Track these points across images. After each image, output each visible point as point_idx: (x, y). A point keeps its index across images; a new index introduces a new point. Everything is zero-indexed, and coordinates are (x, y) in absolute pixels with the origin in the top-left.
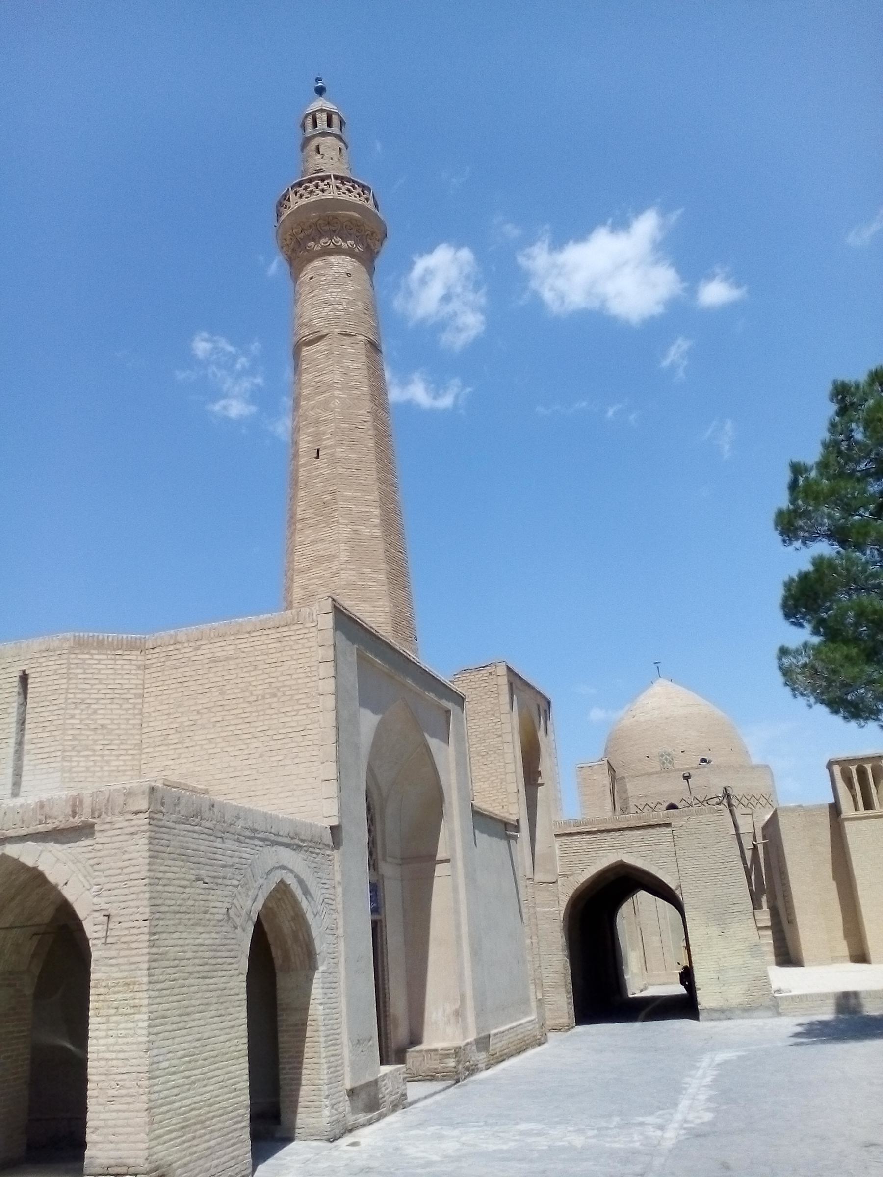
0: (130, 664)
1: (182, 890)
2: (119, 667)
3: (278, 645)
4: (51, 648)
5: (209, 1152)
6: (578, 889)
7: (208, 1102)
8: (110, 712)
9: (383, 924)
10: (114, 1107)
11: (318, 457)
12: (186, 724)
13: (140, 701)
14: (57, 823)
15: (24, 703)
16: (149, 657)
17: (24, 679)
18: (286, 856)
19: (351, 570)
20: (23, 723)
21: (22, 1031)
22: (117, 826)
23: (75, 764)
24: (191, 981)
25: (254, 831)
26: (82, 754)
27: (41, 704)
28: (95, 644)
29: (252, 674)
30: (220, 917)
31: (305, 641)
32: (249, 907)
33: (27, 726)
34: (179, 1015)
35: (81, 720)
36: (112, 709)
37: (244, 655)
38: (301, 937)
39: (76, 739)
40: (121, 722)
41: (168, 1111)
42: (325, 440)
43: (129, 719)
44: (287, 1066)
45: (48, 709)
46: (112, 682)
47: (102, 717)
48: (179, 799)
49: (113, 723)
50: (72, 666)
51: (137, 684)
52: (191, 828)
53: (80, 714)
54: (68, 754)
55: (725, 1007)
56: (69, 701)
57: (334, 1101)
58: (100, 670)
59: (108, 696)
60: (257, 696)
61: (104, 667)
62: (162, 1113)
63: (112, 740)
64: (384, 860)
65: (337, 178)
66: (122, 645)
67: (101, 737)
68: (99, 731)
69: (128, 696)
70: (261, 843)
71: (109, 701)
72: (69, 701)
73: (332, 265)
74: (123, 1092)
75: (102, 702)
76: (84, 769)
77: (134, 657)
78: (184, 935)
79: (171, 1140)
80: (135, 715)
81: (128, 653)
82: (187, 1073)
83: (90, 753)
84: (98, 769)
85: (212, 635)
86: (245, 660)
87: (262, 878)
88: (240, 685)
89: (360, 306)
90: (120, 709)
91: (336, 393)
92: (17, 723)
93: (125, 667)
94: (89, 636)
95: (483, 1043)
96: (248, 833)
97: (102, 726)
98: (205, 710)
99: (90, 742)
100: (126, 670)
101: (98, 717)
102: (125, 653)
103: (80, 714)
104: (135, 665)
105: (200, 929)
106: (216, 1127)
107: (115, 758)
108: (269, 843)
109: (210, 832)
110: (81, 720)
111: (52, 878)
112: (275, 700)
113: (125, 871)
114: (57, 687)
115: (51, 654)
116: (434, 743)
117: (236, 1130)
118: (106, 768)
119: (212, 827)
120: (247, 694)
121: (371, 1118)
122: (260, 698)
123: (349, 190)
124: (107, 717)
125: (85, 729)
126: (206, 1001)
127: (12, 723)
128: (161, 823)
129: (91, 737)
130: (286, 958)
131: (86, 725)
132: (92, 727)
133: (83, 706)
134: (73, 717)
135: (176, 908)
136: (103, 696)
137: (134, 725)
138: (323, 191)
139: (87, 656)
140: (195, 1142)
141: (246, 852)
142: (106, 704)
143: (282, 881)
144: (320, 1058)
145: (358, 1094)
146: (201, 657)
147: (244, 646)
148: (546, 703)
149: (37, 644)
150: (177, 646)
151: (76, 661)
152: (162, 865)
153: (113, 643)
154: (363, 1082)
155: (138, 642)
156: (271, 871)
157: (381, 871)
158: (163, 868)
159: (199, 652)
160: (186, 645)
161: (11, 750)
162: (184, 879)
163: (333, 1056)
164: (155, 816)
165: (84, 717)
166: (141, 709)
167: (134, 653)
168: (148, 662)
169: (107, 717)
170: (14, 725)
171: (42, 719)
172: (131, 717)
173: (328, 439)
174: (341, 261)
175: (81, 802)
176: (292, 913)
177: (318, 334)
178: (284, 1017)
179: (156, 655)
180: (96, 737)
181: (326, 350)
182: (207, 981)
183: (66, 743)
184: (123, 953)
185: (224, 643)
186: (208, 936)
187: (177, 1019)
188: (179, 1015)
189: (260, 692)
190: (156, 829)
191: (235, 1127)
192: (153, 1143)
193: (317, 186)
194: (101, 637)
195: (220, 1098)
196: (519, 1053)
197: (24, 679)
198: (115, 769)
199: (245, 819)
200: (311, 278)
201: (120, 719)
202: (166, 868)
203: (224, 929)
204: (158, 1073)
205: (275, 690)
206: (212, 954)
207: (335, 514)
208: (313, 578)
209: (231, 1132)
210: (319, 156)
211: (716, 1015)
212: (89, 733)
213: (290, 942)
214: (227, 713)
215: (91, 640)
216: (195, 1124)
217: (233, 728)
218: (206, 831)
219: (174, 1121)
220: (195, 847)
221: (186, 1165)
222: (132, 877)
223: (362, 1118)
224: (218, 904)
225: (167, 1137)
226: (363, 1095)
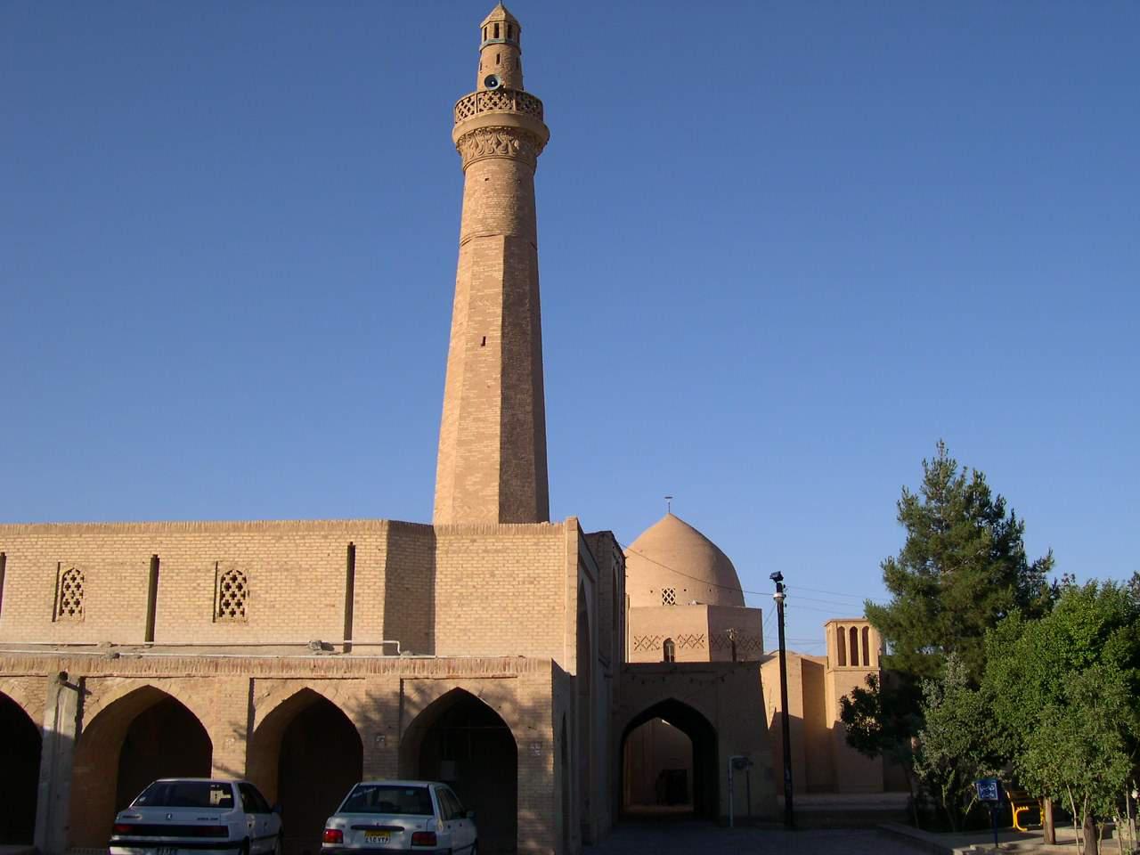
11: (484, 344)
60: (519, 582)
97: (407, 588)
112: (533, 586)
118: (410, 619)
120: (512, 579)
133: (396, 574)
159: (475, 544)
173: (494, 330)
181: (496, 249)
205: (532, 579)
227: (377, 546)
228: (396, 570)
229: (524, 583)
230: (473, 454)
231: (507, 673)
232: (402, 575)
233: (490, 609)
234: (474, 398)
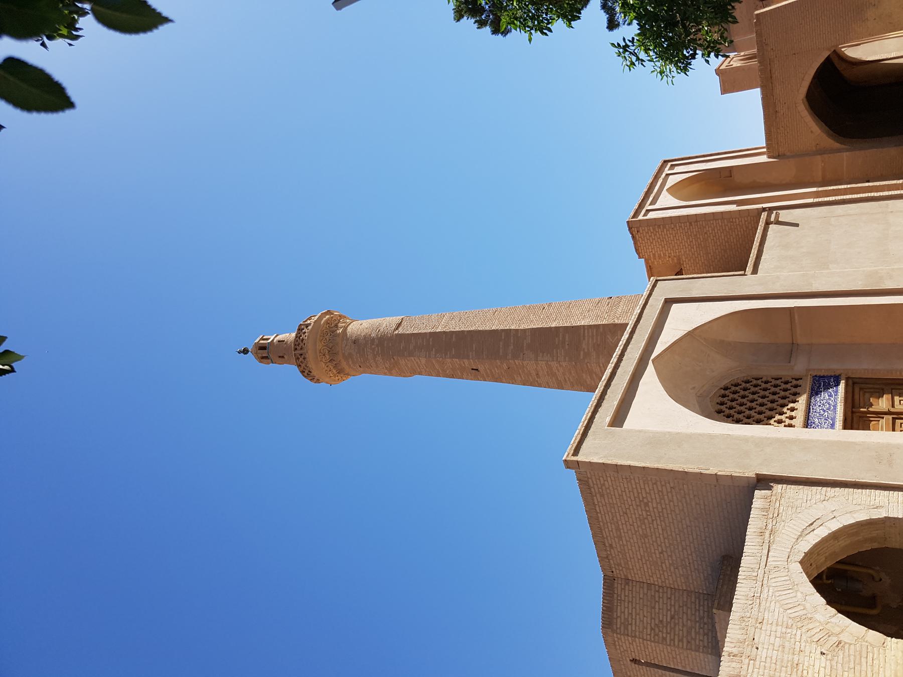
49: (670, 610)
54: (693, 647)
99: (685, 629)
118: (705, 620)
120: (646, 521)
132: (672, 625)
134: (664, 639)
139: (619, 620)
180: (681, 624)
212: (677, 629)
228: (652, 629)
232: (657, 622)
233: (683, 543)
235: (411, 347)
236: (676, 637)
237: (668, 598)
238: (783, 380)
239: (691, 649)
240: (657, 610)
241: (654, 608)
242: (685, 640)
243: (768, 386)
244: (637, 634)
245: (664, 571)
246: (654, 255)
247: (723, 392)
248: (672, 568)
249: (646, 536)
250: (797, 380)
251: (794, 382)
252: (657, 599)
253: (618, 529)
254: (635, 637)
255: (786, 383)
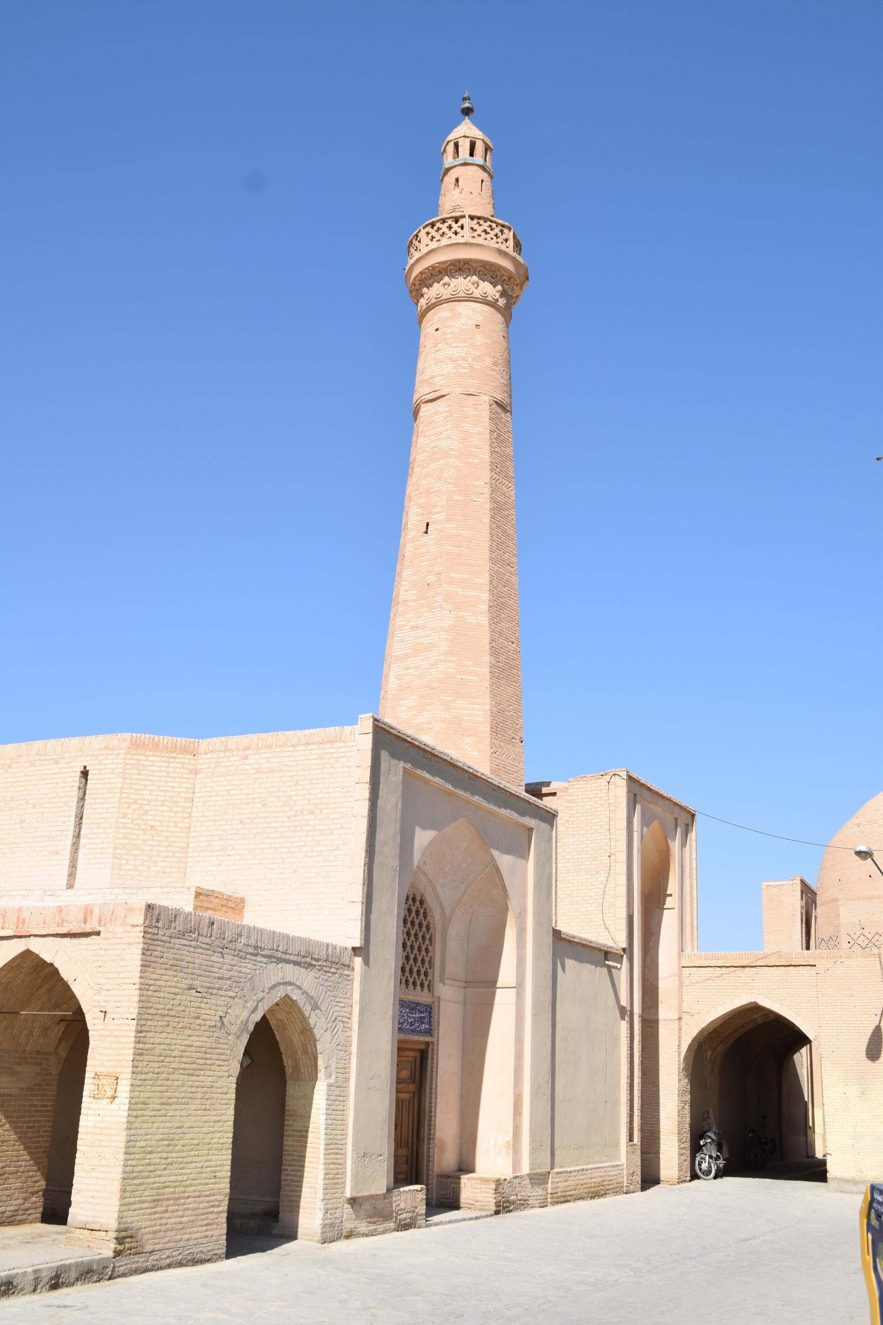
0: (183, 768)
1: (173, 996)
2: (172, 770)
3: (320, 761)
4: (110, 746)
5: (180, 1226)
6: (703, 1030)
7: (184, 1183)
8: (160, 813)
9: (435, 1047)
10: (94, 1175)
12: (229, 832)
13: (189, 805)
14: (72, 927)
15: (83, 799)
16: (201, 761)
17: (85, 774)
18: (290, 972)
19: (450, 661)
20: (81, 818)
21: (46, 1106)
22: (118, 936)
23: (124, 861)
24: (176, 1076)
25: (256, 948)
26: (131, 852)
27: (98, 801)
28: (150, 746)
29: (293, 788)
30: (213, 1023)
31: (345, 760)
32: (245, 1017)
33: (84, 821)
34: (161, 1104)
35: (133, 820)
36: (162, 812)
37: (287, 768)
38: (310, 1051)
39: (127, 838)
40: (171, 824)
41: (141, 1184)
42: (435, 513)
43: (178, 822)
44: (290, 1168)
45: (104, 806)
46: (163, 784)
47: (152, 818)
48: (176, 916)
50: (128, 766)
51: (188, 788)
52: (187, 943)
53: (132, 814)
54: (118, 851)
55: (858, 1179)
56: (123, 800)
57: (329, 1206)
58: (153, 771)
59: (160, 798)
61: (157, 769)
62: (135, 1184)
63: (160, 841)
64: (442, 981)
65: (472, 218)
66: (176, 748)
67: (150, 838)
68: (149, 832)
69: (179, 799)
70: (265, 960)
71: (160, 803)
72: (123, 800)
73: (459, 316)
74: (104, 1163)
75: (152, 803)
76: (132, 867)
77: (187, 761)
78: (171, 1036)
79: (141, 1209)
80: (183, 818)
81: (182, 756)
82: (164, 1155)
83: (140, 853)
84: (145, 868)
85: (260, 746)
86: (288, 774)
87: (263, 991)
88: (281, 799)
89: (488, 361)
90: (170, 811)
91: (451, 461)
92: (76, 816)
93: (177, 770)
94: (144, 739)
95: (538, 1179)
96: (251, 950)
98: (248, 821)
100: (178, 773)
101: (149, 818)
102: (178, 756)
103: (132, 814)
104: (187, 768)
105: (187, 1032)
106: (191, 1206)
107: (162, 859)
108: (275, 960)
109: (208, 947)
110: (133, 820)
111: (64, 974)
112: (313, 817)
113: (121, 975)
114: (113, 785)
115: (109, 752)
116: (504, 861)
117: (212, 1213)
118: (153, 868)
119: (210, 942)
120: (287, 808)
121: (375, 1230)
122: (298, 813)
123: (485, 231)
124: (157, 818)
125: (136, 829)
126: (190, 1095)
127: (71, 816)
128: (156, 937)
129: (140, 837)
130: (296, 1068)
131: (137, 825)
132: (143, 827)
134: (125, 816)
135: (166, 1012)
136: (154, 798)
137: (183, 828)
138: (456, 233)
139: (143, 758)
140: (166, 1215)
141: (247, 967)
142: (157, 806)
143: (287, 996)
144: (318, 1163)
145: (360, 1205)
146: (248, 767)
147: (288, 759)
148: (690, 816)
149: (98, 741)
150: (228, 754)
151: (132, 762)
152: (154, 973)
153: (167, 745)
154: (366, 1194)
155: (192, 745)
156: (274, 986)
157: (436, 994)
158: (153, 976)
159: (247, 762)
160: (235, 753)
161: (69, 842)
162: (176, 987)
163: (333, 1163)
164: (150, 930)
165: (135, 817)
166: (190, 813)
167: (187, 756)
168: (199, 767)
169: (157, 818)
170: (73, 818)
171: (97, 816)
172: (180, 820)
174: (470, 312)
175: (91, 912)
176: (301, 1027)
177: (438, 394)
178: (291, 1122)
179: (208, 761)
180: (145, 837)
182: (194, 1078)
183: (117, 841)
184: (113, 1045)
185: (270, 755)
186: (197, 1038)
187: (159, 1107)
188: (161, 1104)
189: (299, 808)
190: (149, 941)
191: (212, 1209)
192: (125, 1208)
193: (450, 227)
194: (156, 739)
195: (198, 1182)
196: (593, 1198)
197: (85, 774)
198: (162, 869)
199: (248, 937)
200: (437, 330)
201: (169, 821)
202: (157, 977)
203: (215, 1034)
204: (134, 1150)
206: (201, 1055)
207: (439, 598)
208: (409, 668)
209: (207, 1213)
210: (458, 190)
211: (848, 1187)
213: (299, 1054)
214: (267, 825)
215: (147, 741)
216: (168, 1199)
217: (272, 841)
218: (203, 946)
219: (146, 1193)
220: (190, 959)
221: (155, 1232)
222: (126, 981)
223: (363, 1227)
224: (211, 1011)
225: (137, 1206)
226: (367, 1206)
227: (113, 769)
228: (136, 801)
229: (302, 813)
230: (408, 671)
231: (88, 928)
232: (146, 807)
234: (414, 601)
235: (467, 426)
236: (129, 831)
237: (177, 822)
238: (429, 970)
239: (116, 849)
240: (160, 808)
241: (162, 805)
242: (126, 841)
243: (423, 952)
244: (128, 781)
245: (215, 821)
246: (573, 801)
247: (418, 899)
248: (219, 833)
249: (265, 805)
250: (429, 986)
251: (426, 984)
252: (174, 809)
253: (272, 771)
254: (125, 778)
255: (426, 974)
